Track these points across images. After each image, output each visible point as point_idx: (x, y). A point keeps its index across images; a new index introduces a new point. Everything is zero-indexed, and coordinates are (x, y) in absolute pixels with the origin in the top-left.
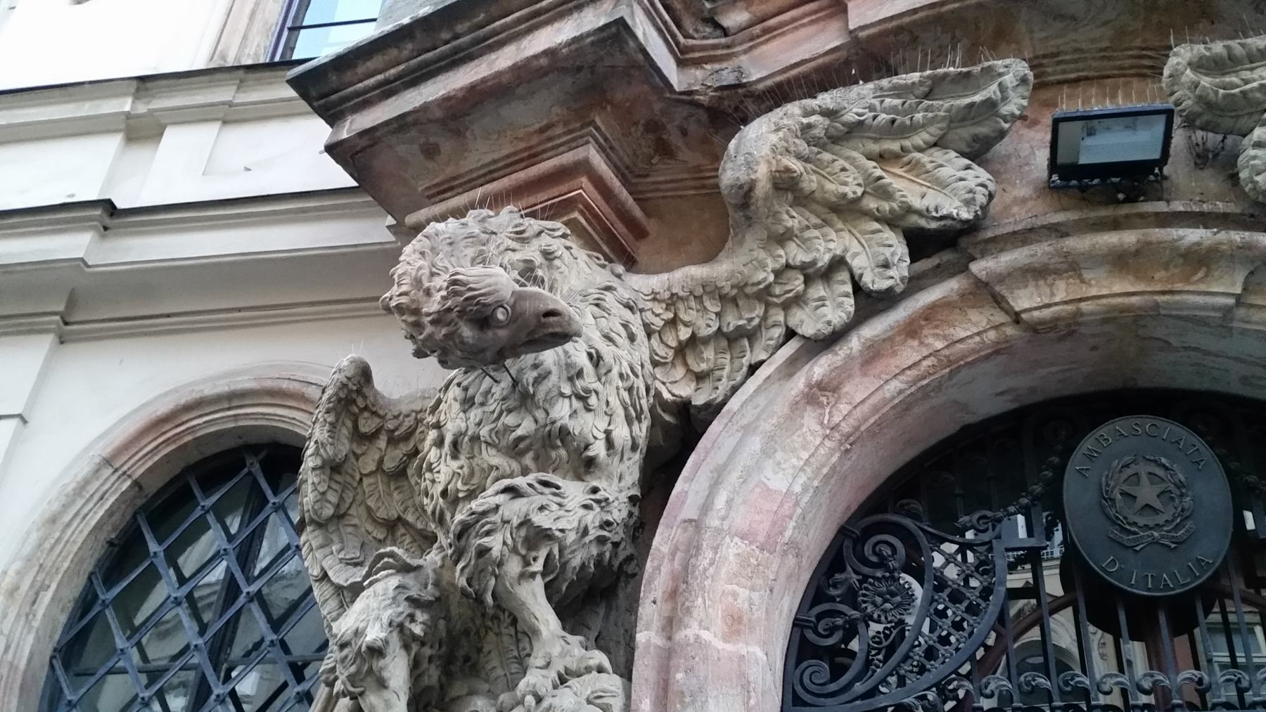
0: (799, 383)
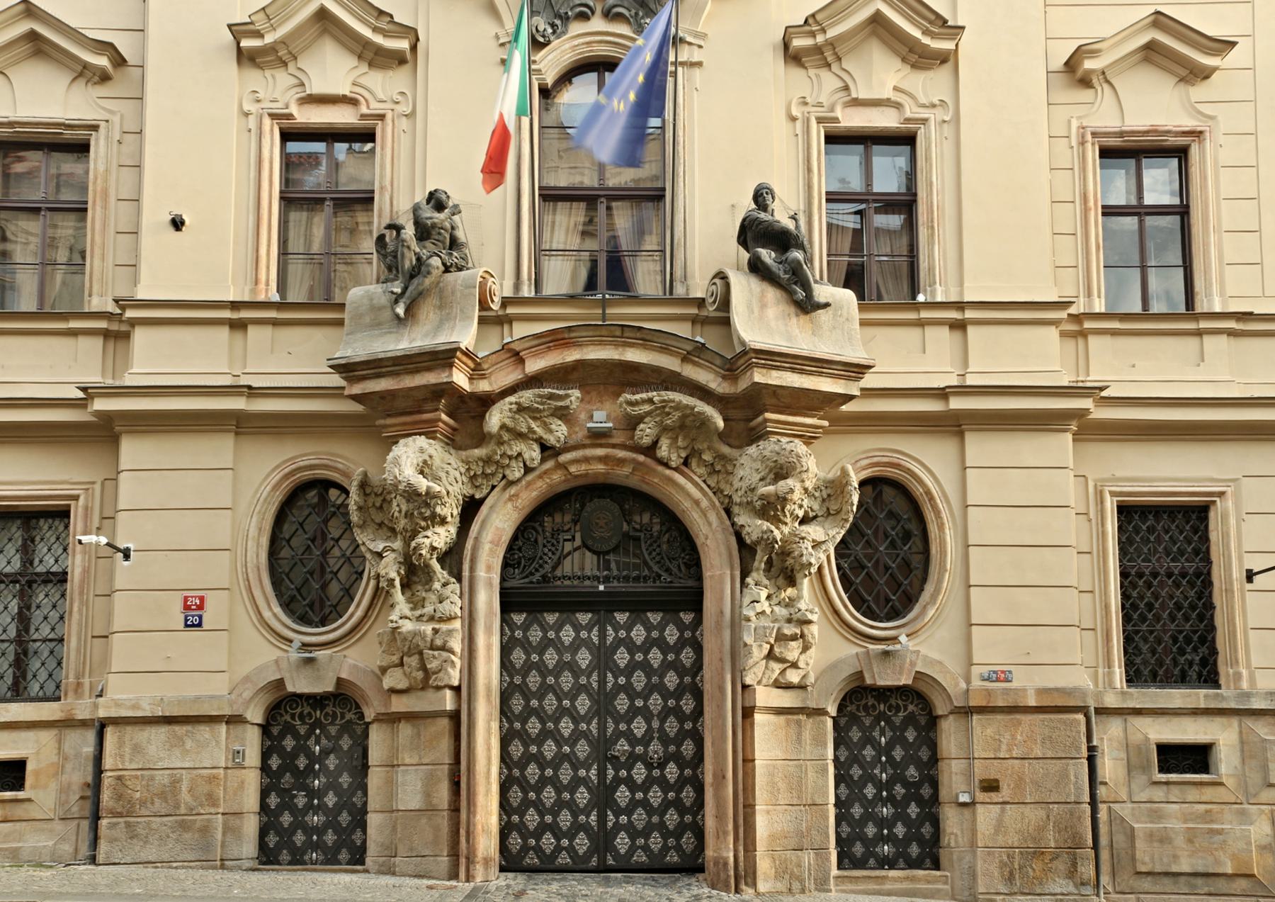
0: (507, 495)
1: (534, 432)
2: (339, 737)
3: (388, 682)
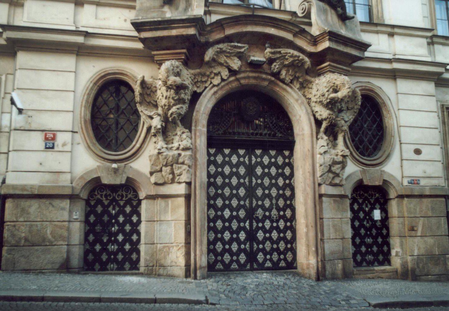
1: (227, 63)
2: (125, 206)
3: (153, 179)
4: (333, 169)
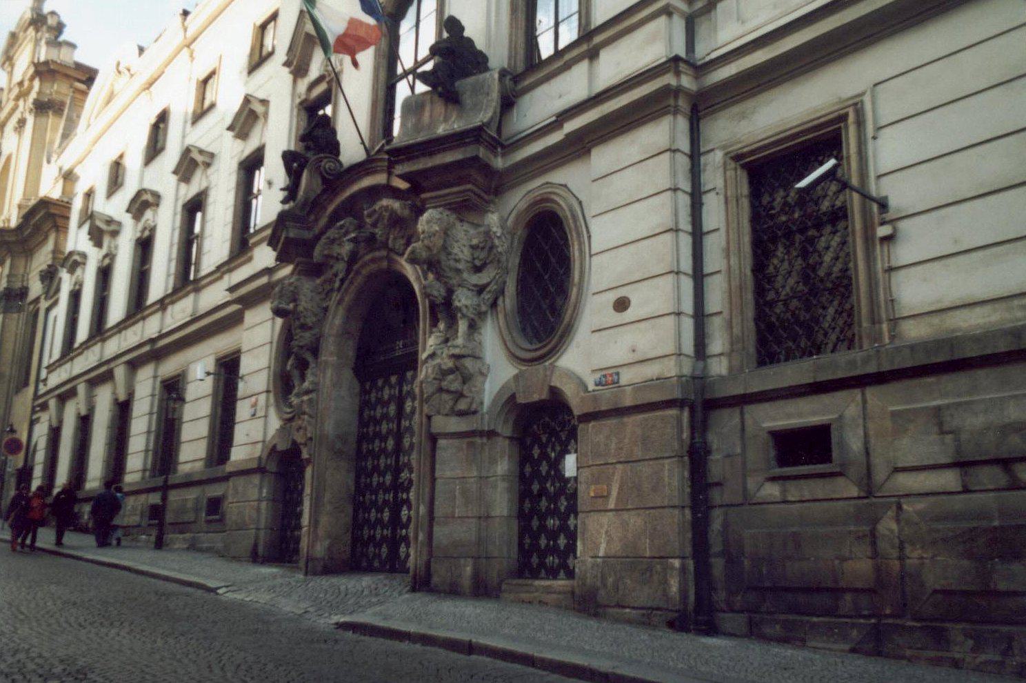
4: (444, 384)
